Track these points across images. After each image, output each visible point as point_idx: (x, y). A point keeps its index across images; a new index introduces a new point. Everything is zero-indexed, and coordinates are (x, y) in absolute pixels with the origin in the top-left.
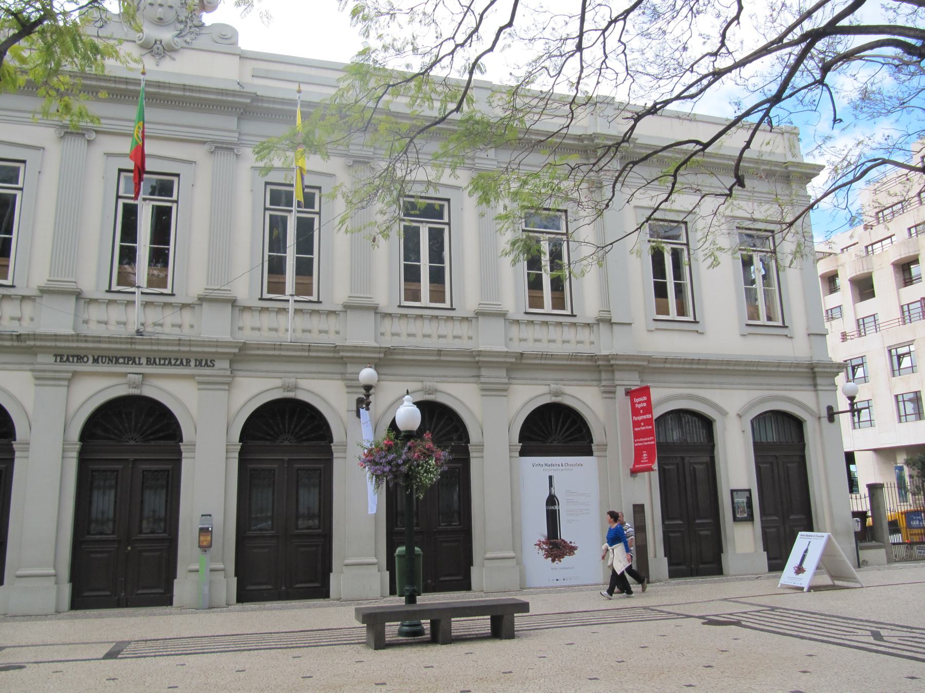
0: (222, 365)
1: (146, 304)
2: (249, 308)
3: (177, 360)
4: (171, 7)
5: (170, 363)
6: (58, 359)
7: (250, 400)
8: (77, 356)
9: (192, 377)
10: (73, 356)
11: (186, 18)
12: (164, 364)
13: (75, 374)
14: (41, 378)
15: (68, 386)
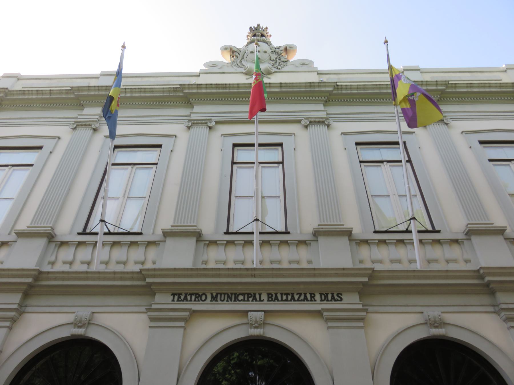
0: (351, 301)
1: (263, 243)
2: (366, 242)
3: (300, 294)
4: (265, 52)
5: (293, 298)
6: (176, 298)
7: (399, 334)
8: (195, 294)
9: (319, 313)
10: (191, 295)
11: (276, 58)
12: (287, 300)
13: (194, 313)
14: (157, 319)
15: (185, 328)
